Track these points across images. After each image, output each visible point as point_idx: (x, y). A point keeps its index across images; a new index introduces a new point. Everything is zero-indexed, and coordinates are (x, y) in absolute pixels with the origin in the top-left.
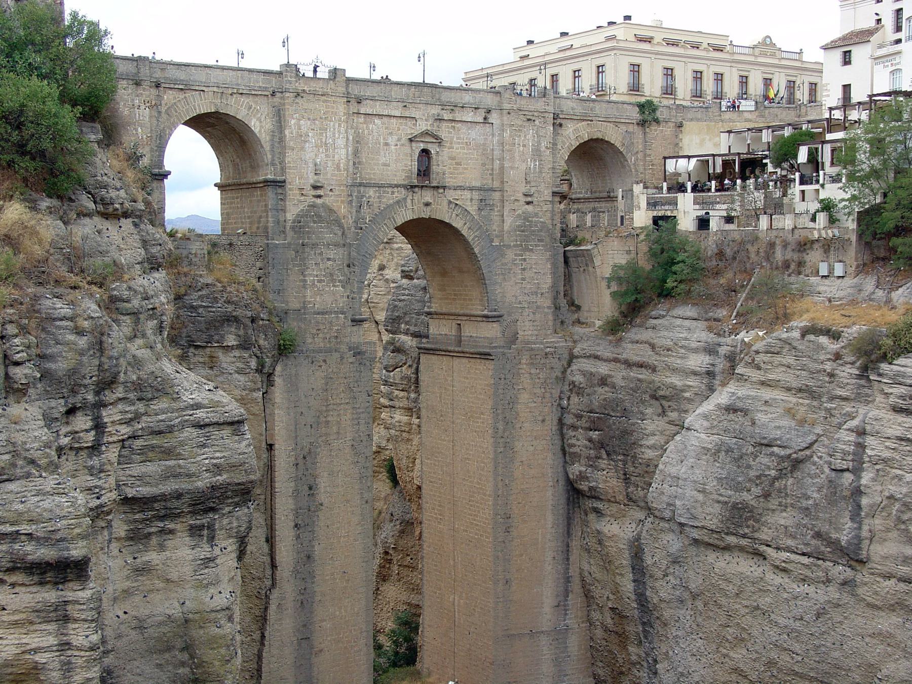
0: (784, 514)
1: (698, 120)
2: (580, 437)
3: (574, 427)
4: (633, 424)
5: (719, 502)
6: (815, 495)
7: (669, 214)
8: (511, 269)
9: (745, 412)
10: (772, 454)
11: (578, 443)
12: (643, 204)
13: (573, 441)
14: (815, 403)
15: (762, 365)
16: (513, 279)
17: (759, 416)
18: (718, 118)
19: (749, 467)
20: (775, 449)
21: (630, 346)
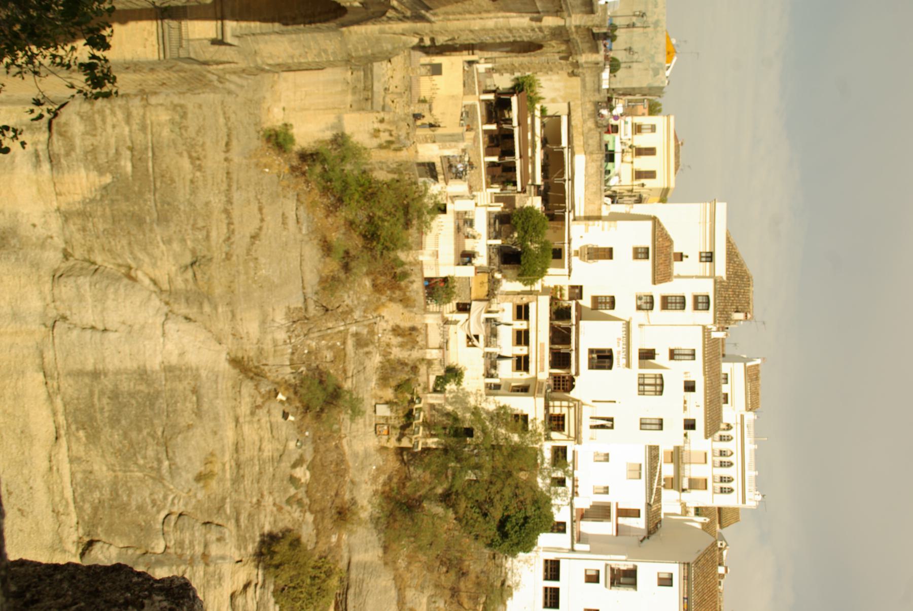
0: (105, 468)
1: (584, 86)
2: (117, 130)
3: (128, 118)
4: (151, 230)
5: (92, 394)
6: (134, 504)
7: (440, 177)
8: (309, 48)
9: (198, 412)
10: (160, 461)
11: (109, 129)
12: (448, 152)
13: (110, 120)
14: (228, 484)
15: (256, 419)
16: (297, 52)
17: (198, 431)
18: (587, 99)
19: (140, 430)
20: (166, 463)
21: (252, 194)
